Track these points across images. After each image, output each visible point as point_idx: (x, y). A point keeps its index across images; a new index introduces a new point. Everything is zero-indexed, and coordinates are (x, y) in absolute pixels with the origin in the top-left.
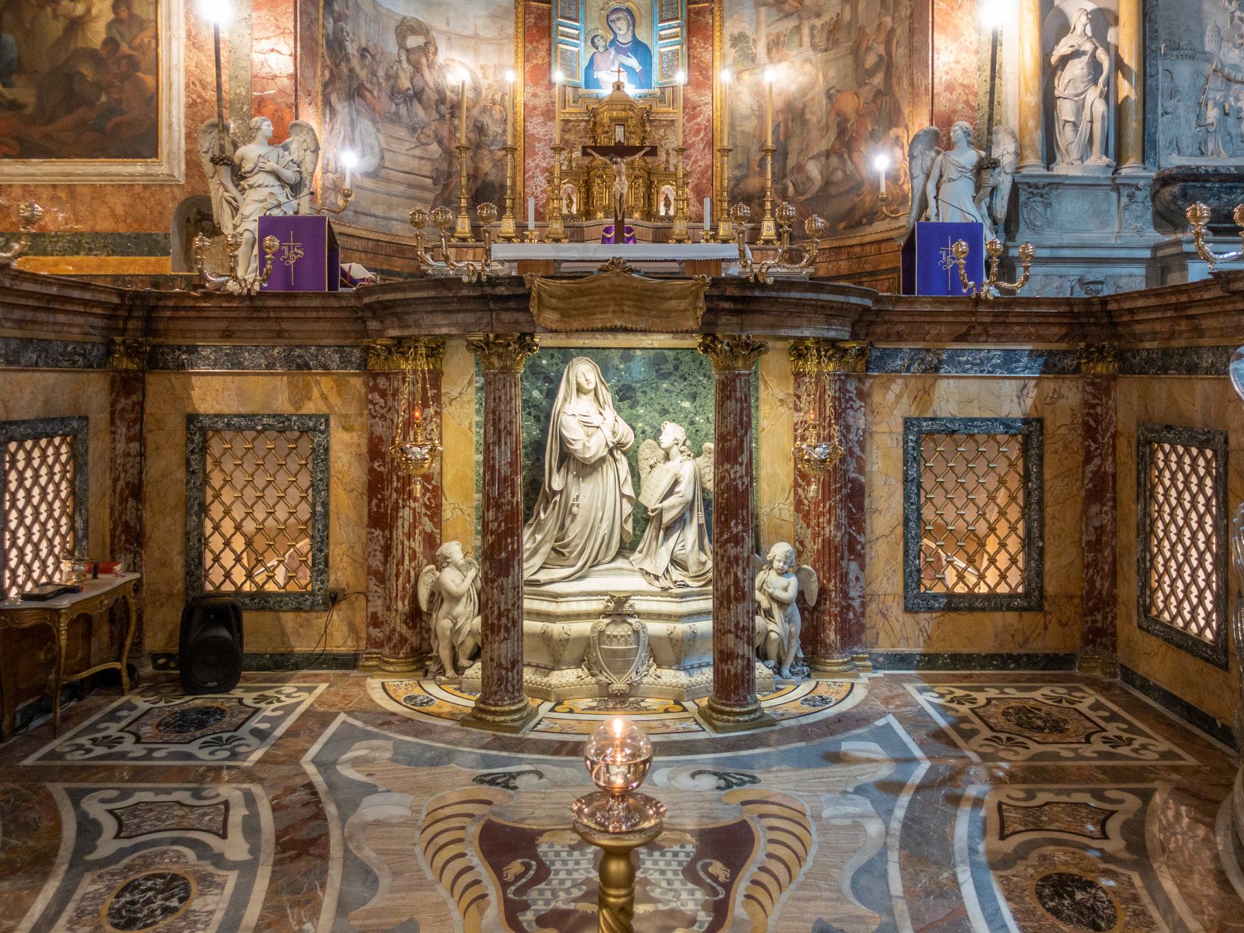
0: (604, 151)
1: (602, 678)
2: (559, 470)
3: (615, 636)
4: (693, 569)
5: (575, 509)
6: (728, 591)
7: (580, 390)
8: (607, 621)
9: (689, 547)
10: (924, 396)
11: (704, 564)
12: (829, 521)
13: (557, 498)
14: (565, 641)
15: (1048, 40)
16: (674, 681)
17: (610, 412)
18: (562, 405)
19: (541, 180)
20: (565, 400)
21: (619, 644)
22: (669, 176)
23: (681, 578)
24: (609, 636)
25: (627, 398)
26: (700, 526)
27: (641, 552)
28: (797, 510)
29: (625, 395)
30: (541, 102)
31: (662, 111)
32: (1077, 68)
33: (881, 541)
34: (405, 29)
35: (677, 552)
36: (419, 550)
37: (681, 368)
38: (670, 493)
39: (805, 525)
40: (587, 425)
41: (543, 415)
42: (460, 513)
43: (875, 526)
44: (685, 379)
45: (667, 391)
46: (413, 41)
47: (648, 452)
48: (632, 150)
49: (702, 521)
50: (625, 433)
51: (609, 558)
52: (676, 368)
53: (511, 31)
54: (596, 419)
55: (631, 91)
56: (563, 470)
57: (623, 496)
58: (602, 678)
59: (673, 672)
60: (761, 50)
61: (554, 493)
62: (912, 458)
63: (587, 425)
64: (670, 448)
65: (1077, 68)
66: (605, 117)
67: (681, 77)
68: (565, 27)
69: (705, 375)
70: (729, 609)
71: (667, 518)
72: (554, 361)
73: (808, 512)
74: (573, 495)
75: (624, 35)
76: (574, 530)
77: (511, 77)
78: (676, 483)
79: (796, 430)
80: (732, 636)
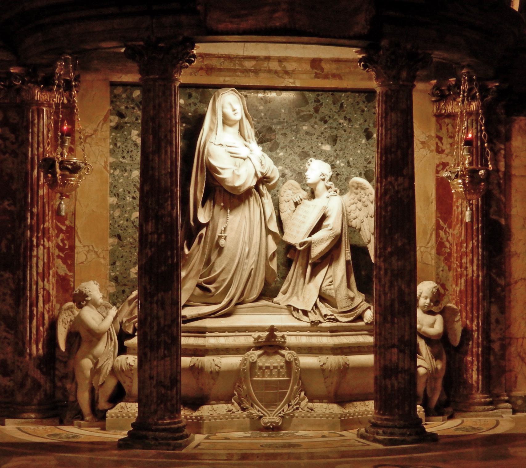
1: (254, 411)
2: (203, 205)
3: (268, 368)
4: (343, 304)
5: (222, 242)
6: (392, 305)
7: (226, 121)
8: (259, 352)
9: (337, 283)
11: (352, 299)
12: (472, 262)
13: (203, 231)
14: (216, 374)
16: (328, 411)
17: (254, 144)
18: (208, 136)
20: (211, 130)
21: (271, 375)
23: (329, 313)
24: (261, 368)
25: (268, 140)
26: (347, 262)
27: (285, 293)
28: (439, 253)
33: (519, 284)
35: (325, 287)
36: (53, 292)
37: (322, 110)
38: (318, 227)
39: (447, 268)
40: (234, 155)
42: (94, 256)
43: (514, 269)
44: (326, 122)
45: (307, 133)
49: (349, 258)
51: (254, 295)
52: (317, 110)
54: (243, 152)
56: (208, 204)
57: (268, 232)
58: (254, 411)
59: (325, 405)
61: (200, 226)
63: (234, 155)
64: (316, 184)
69: (345, 118)
70: (393, 323)
71: (316, 251)
72: (192, 101)
73: (450, 254)
74: (220, 227)
76: (220, 265)
78: (324, 217)
79: (438, 172)
80: (395, 350)
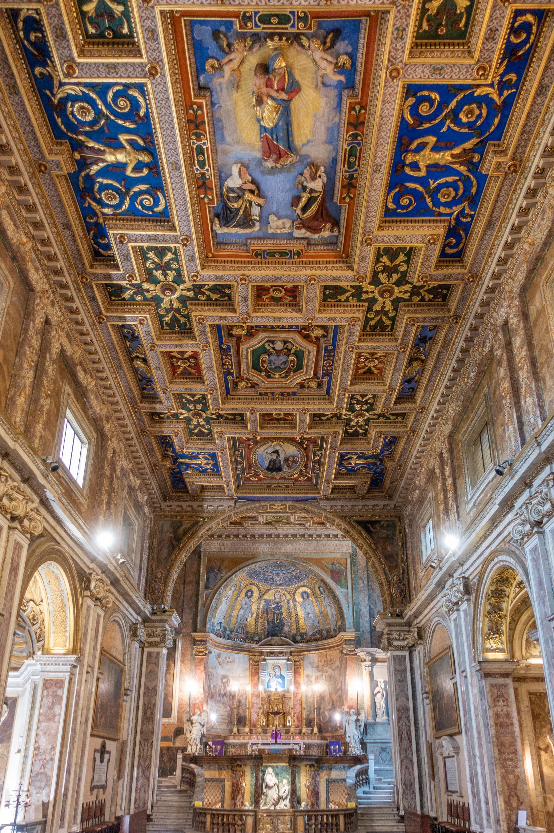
0: (272, 713)
10: (329, 775)
15: (372, 690)
19: (255, 715)
22: (289, 714)
29: (277, 775)
30: (256, 693)
31: (288, 695)
32: (379, 695)
34: (224, 677)
41: (263, 779)
46: (224, 680)
47: (281, 785)
48: (279, 713)
50: (277, 782)
53: (248, 673)
55: (280, 689)
60: (313, 679)
62: (327, 787)
65: (379, 696)
66: (273, 698)
67: (292, 688)
68: (262, 673)
75: (278, 673)
77: (249, 688)
